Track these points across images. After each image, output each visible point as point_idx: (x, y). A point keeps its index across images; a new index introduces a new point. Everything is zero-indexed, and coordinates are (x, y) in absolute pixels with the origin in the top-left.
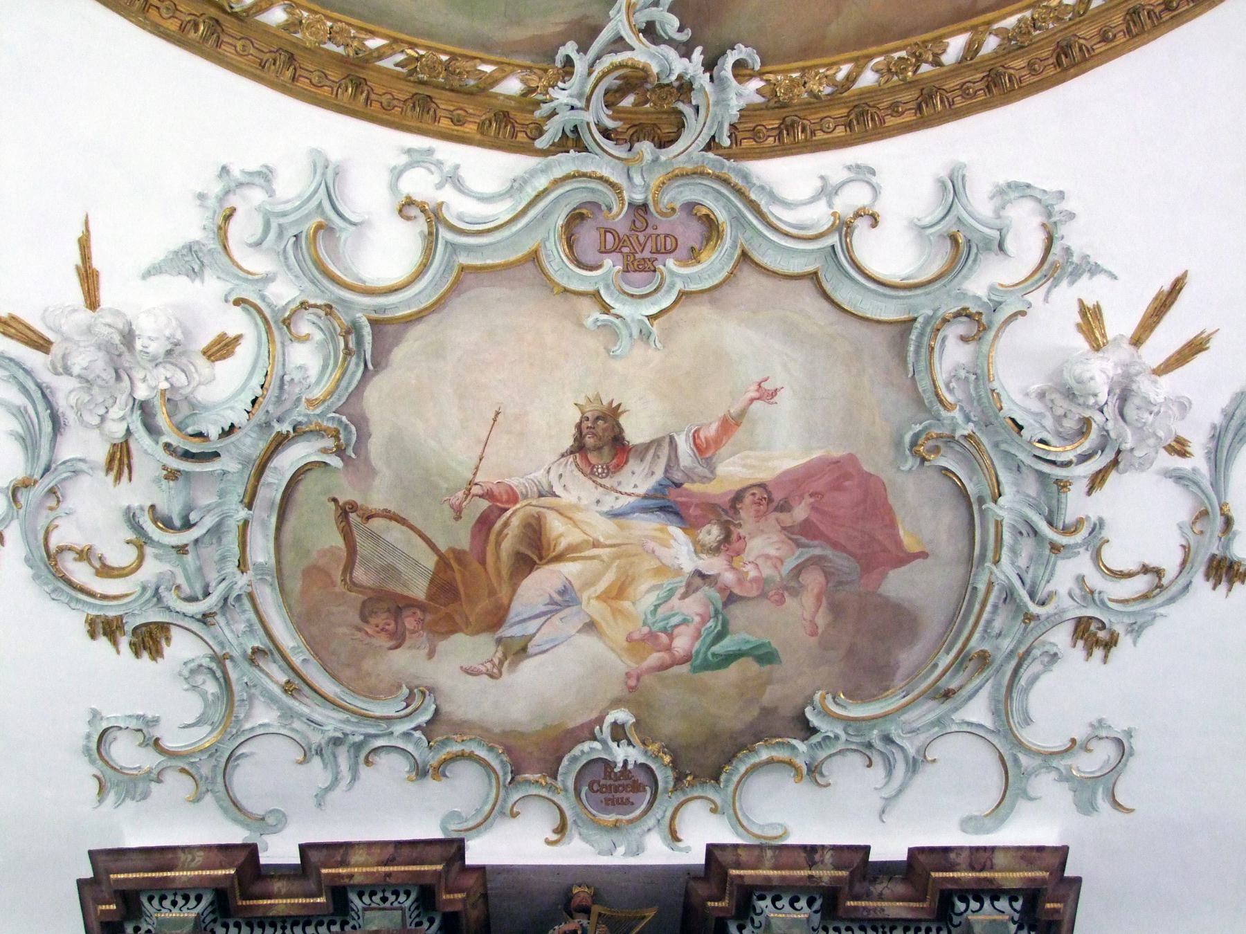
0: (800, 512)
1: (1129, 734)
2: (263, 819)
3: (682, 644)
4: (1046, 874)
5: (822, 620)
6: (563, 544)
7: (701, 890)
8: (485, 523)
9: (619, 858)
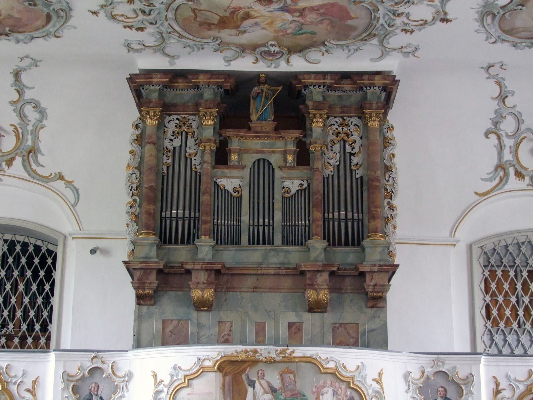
0: (322, 11)
1: (418, 46)
2: (174, 56)
3: (289, 31)
4: (389, 82)
5: (329, 28)
6: (255, 16)
7: (294, 82)
8: (233, 13)
9: (272, 69)
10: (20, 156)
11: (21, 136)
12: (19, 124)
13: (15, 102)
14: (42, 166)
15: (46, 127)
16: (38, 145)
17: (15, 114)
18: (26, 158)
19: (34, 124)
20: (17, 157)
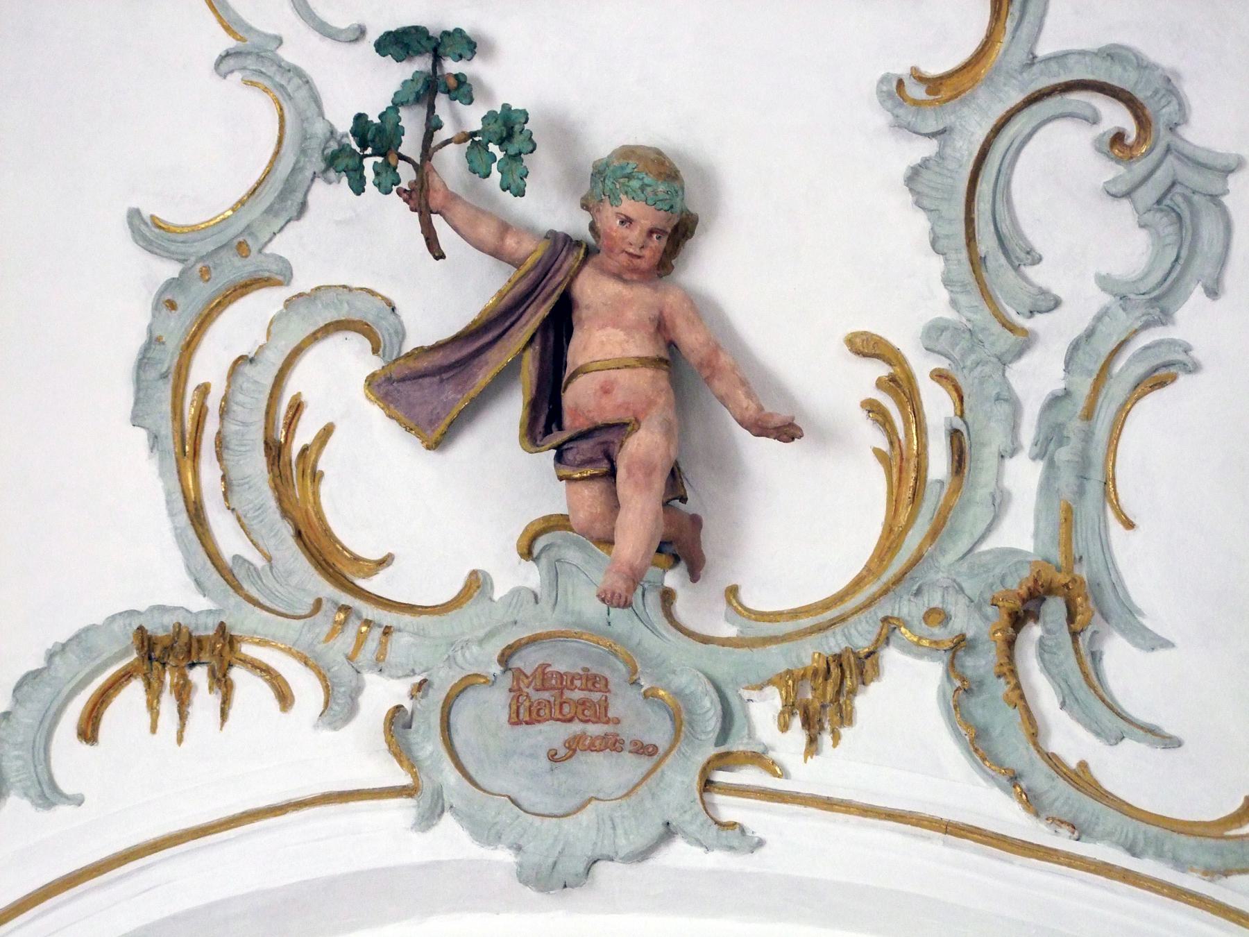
10: (915, 649)
11: (939, 464)
12: (935, 335)
13: (934, 84)
14: (1153, 734)
15: (1193, 368)
16: (1105, 547)
17: (920, 224)
18: (982, 663)
19: (1090, 334)
20: (891, 657)
